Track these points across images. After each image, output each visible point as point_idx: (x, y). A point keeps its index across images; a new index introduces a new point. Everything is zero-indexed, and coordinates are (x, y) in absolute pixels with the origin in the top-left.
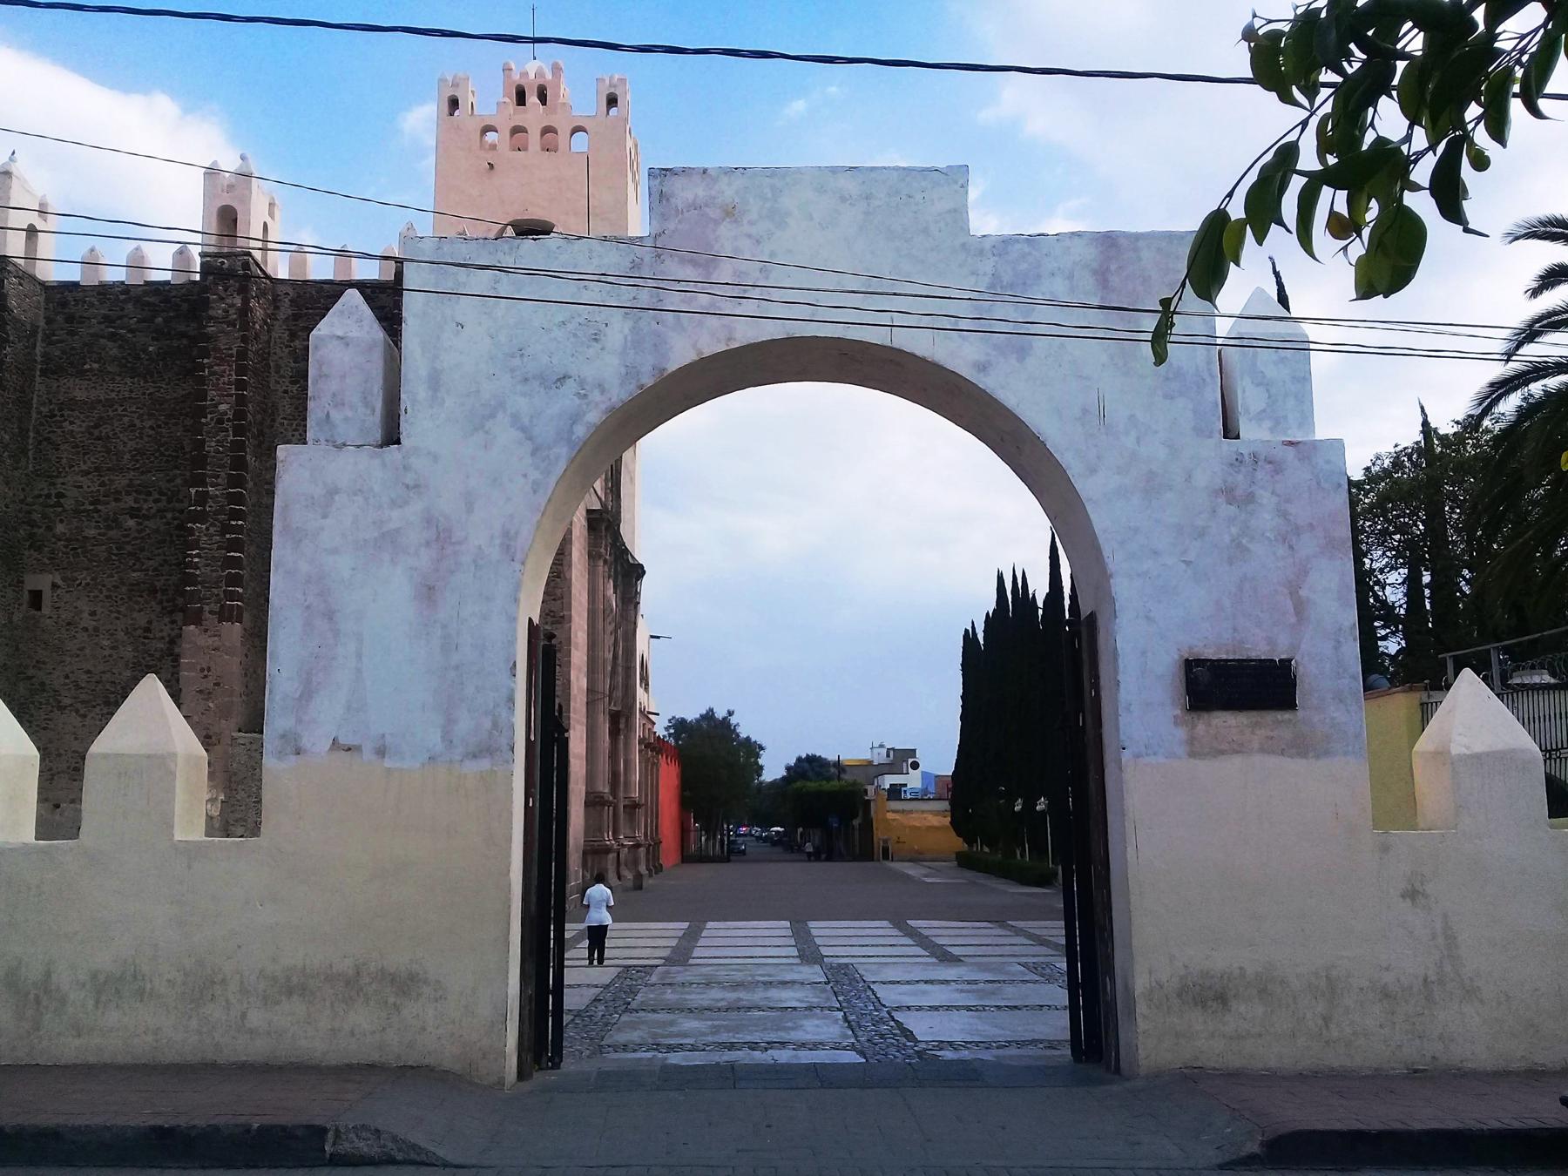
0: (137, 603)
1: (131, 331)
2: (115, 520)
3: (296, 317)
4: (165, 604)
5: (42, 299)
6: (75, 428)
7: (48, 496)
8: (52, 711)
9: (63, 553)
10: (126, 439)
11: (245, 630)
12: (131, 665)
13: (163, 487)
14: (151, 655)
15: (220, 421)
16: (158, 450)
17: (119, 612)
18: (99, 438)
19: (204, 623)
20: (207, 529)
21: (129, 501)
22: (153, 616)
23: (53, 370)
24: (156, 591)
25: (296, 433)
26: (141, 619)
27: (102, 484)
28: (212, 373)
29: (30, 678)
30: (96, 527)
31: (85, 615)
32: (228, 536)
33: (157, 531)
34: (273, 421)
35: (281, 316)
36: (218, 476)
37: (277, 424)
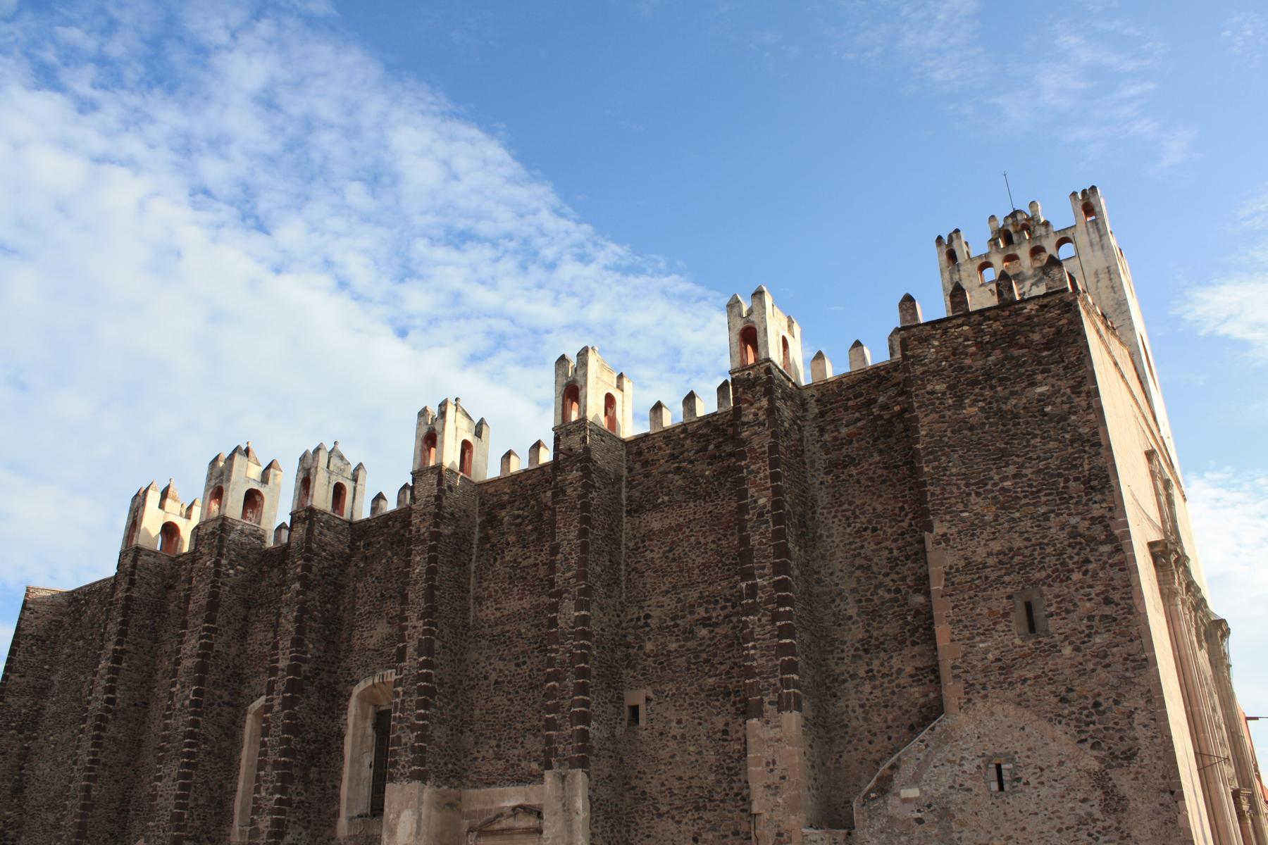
0: (715, 707)
1: (691, 462)
2: (691, 632)
3: (822, 414)
4: (739, 705)
5: (624, 453)
6: (656, 556)
7: (638, 619)
8: (652, 819)
9: (654, 668)
10: (694, 557)
11: (806, 719)
12: (714, 769)
13: (728, 594)
14: (730, 757)
15: (761, 515)
16: (721, 561)
17: (700, 718)
18: (674, 560)
19: (765, 714)
20: (759, 620)
21: (701, 612)
22: (729, 719)
23: (635, 510)
24: (729, 694)
25: (836, 520)
26: (719, 722)
27: (679, 601)
28: (750, 473)
29: (634, 788)
30: (678, 641)
31: (674, 724)
32: (778, 624)
33: (726, 636)
34: (814, 512)
35: (810, 416)
36: (764, 568)
37: (818, 515)
